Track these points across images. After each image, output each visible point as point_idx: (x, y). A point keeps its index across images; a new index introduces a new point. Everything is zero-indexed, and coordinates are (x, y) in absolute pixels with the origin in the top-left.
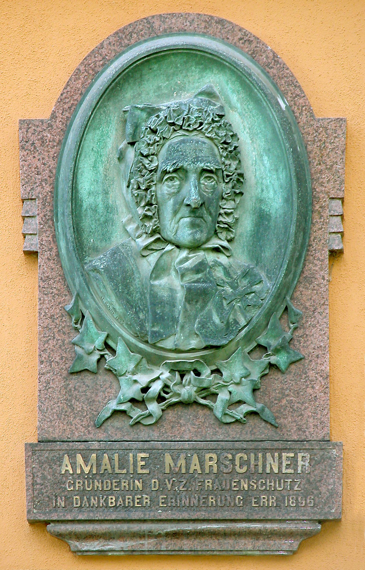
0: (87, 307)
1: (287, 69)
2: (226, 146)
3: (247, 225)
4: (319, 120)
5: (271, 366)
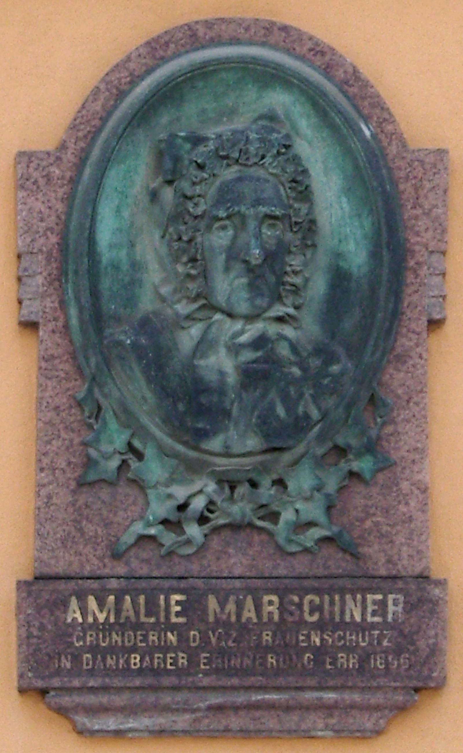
0: (106, 396)
1: (372, 87)
2: (294, 185)
3: (319, 286)
4: (413, 151)
5: (352, 474)
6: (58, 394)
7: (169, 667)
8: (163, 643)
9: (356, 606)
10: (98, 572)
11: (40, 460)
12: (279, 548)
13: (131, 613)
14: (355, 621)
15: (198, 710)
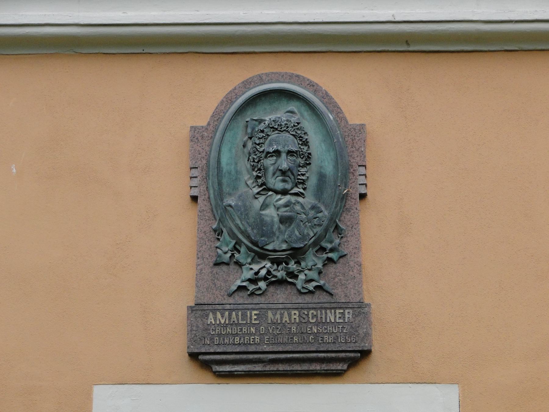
0: (224, 227)
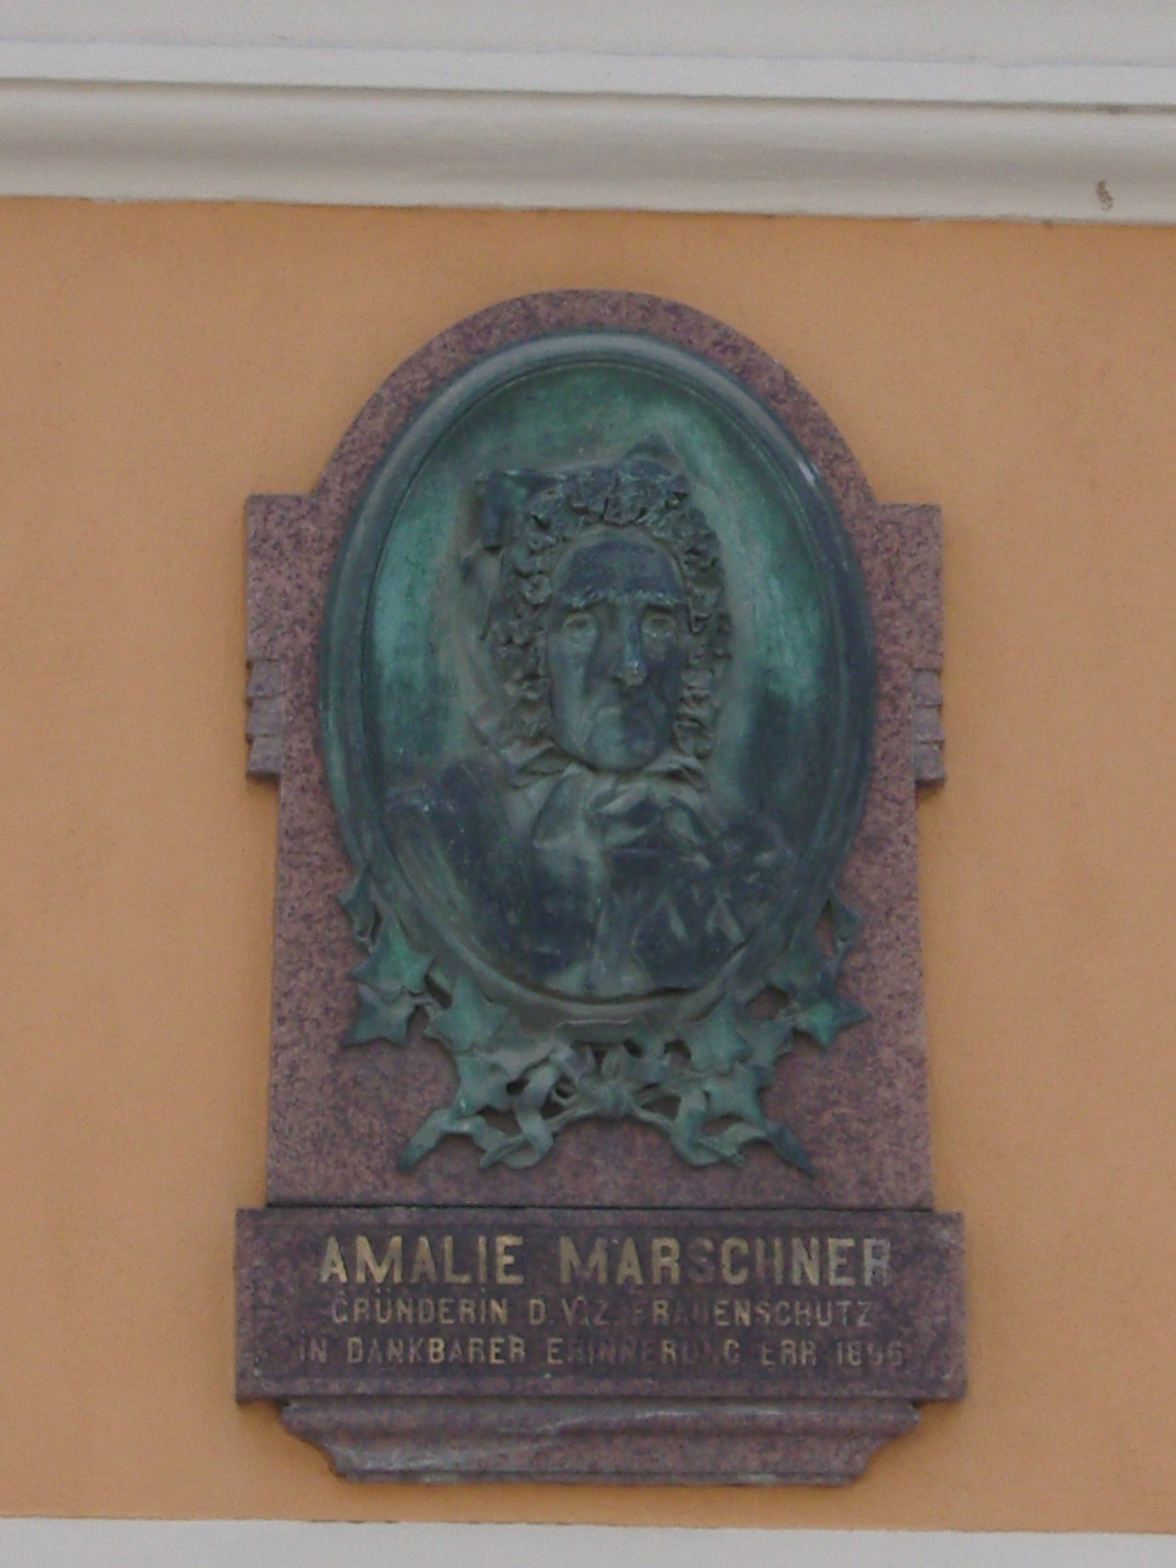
0: (389, 898)
6: (309, 893)
7: (493, 1360)
8: (483, 1319)
9: (810, 1258)
10: (375, 1195)
11: (279, 1005)
12: (678, 1157)
13: (430, 1268)
14: (810, 1284)
15: (543, 1435)
